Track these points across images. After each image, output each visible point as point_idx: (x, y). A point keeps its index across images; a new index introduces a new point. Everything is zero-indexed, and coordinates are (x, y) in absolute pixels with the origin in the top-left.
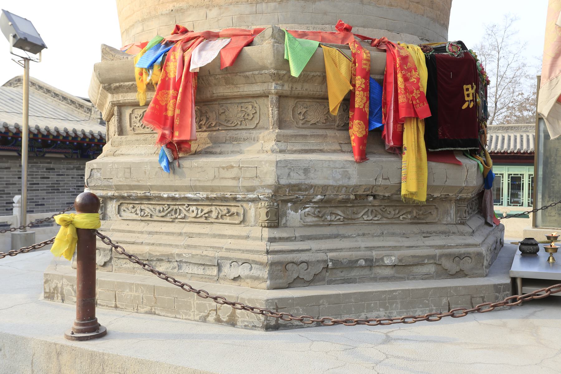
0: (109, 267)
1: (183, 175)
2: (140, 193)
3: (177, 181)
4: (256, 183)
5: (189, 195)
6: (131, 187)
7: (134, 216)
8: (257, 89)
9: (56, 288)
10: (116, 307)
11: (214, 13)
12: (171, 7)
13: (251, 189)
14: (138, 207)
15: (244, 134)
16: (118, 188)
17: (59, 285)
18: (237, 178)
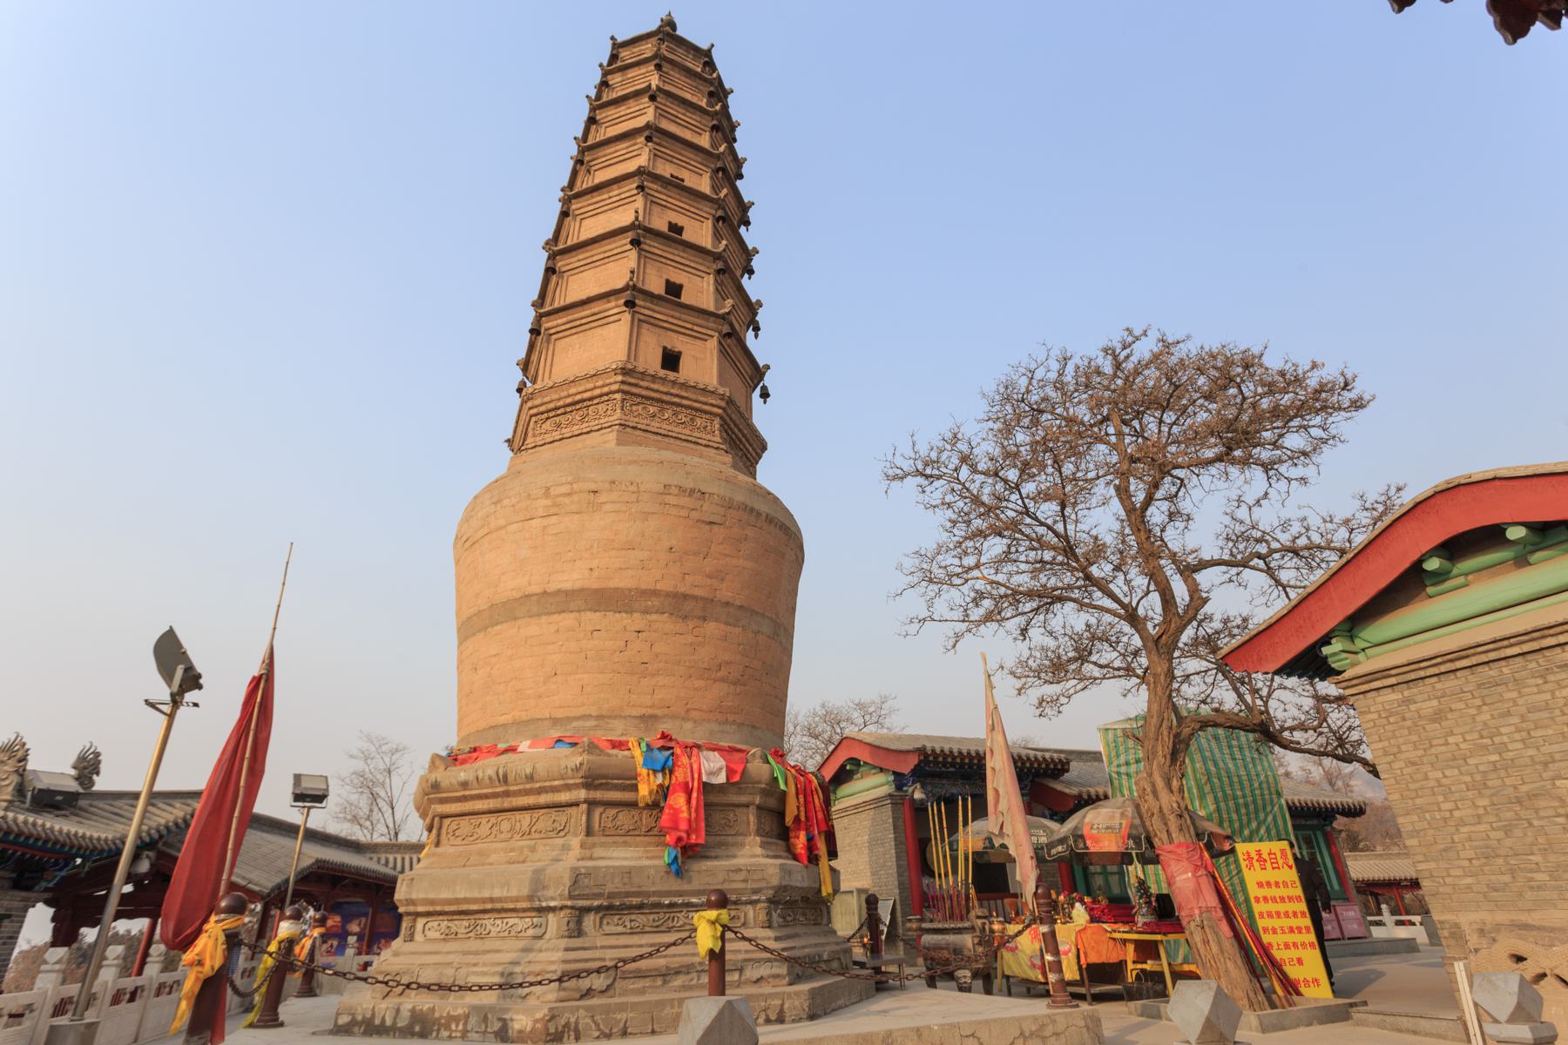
0: (611, 992)
1: (690, 882)
2: (635, 901)
3: (686, 887)
4: (763, 884)
5: (694, 900)
6: (628, 894)
7: (620, 929)
8: (743, 799)
9: (567, 1025)
10: (653, 1032)
11: (689, 725)
12: (643, 711)
13: (756, 891)
14: (627, 919)
15: (730, 839)
16: (611, 896)
17: (573, 1020)
18: (745, 881)
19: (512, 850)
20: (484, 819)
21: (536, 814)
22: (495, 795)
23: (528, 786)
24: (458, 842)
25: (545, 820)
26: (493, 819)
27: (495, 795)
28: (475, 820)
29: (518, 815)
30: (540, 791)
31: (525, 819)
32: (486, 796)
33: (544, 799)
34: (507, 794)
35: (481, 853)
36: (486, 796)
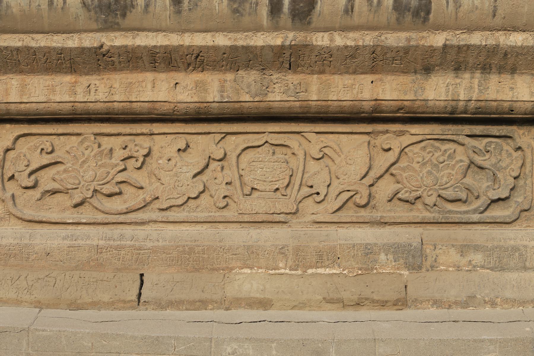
19: (325, 256)
20: (165, 142)
21: (396, 138)
22: (234, 60)
23: (394, 39)
24: (56, 209)
25: (431, 162)
26: (205, 142)
27: (234, 60)
28: (117, 141)
29: (312, 139)
30: (426, 63)
31: (351, 151)
32: (198, 60)
33: (438, 90)
34: (289, 59)
35: (194, 260)
36: (198, 60)
